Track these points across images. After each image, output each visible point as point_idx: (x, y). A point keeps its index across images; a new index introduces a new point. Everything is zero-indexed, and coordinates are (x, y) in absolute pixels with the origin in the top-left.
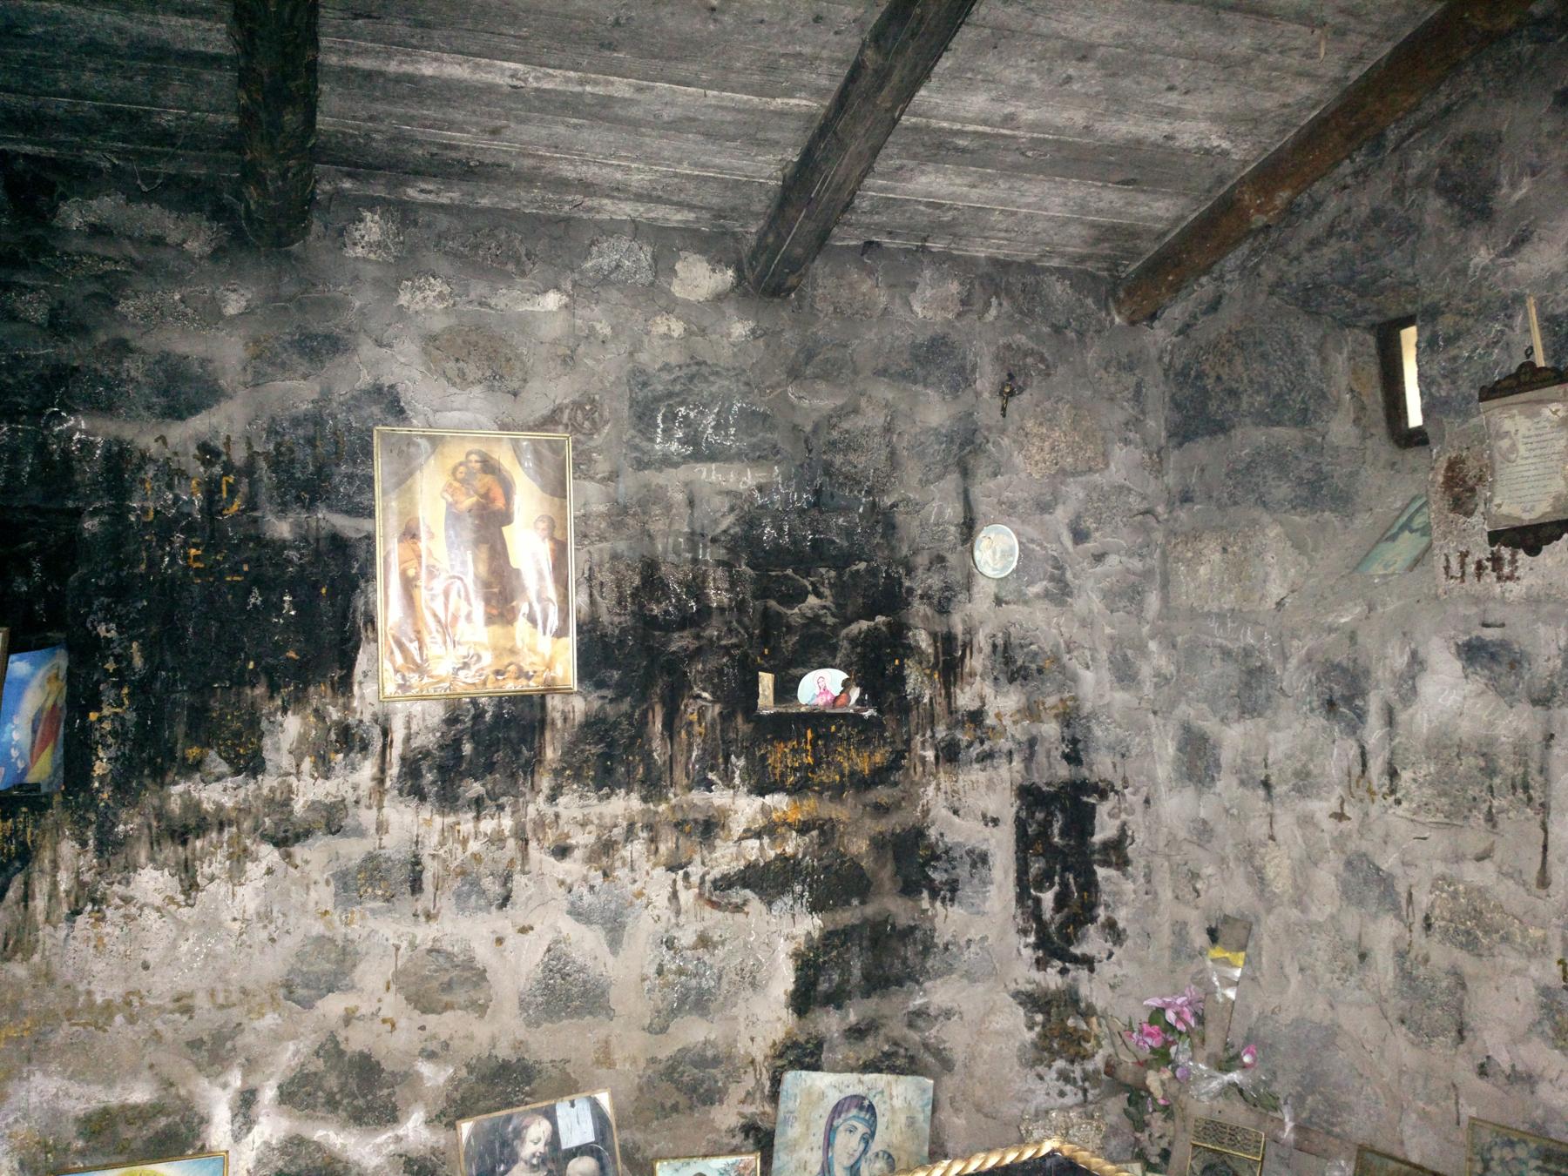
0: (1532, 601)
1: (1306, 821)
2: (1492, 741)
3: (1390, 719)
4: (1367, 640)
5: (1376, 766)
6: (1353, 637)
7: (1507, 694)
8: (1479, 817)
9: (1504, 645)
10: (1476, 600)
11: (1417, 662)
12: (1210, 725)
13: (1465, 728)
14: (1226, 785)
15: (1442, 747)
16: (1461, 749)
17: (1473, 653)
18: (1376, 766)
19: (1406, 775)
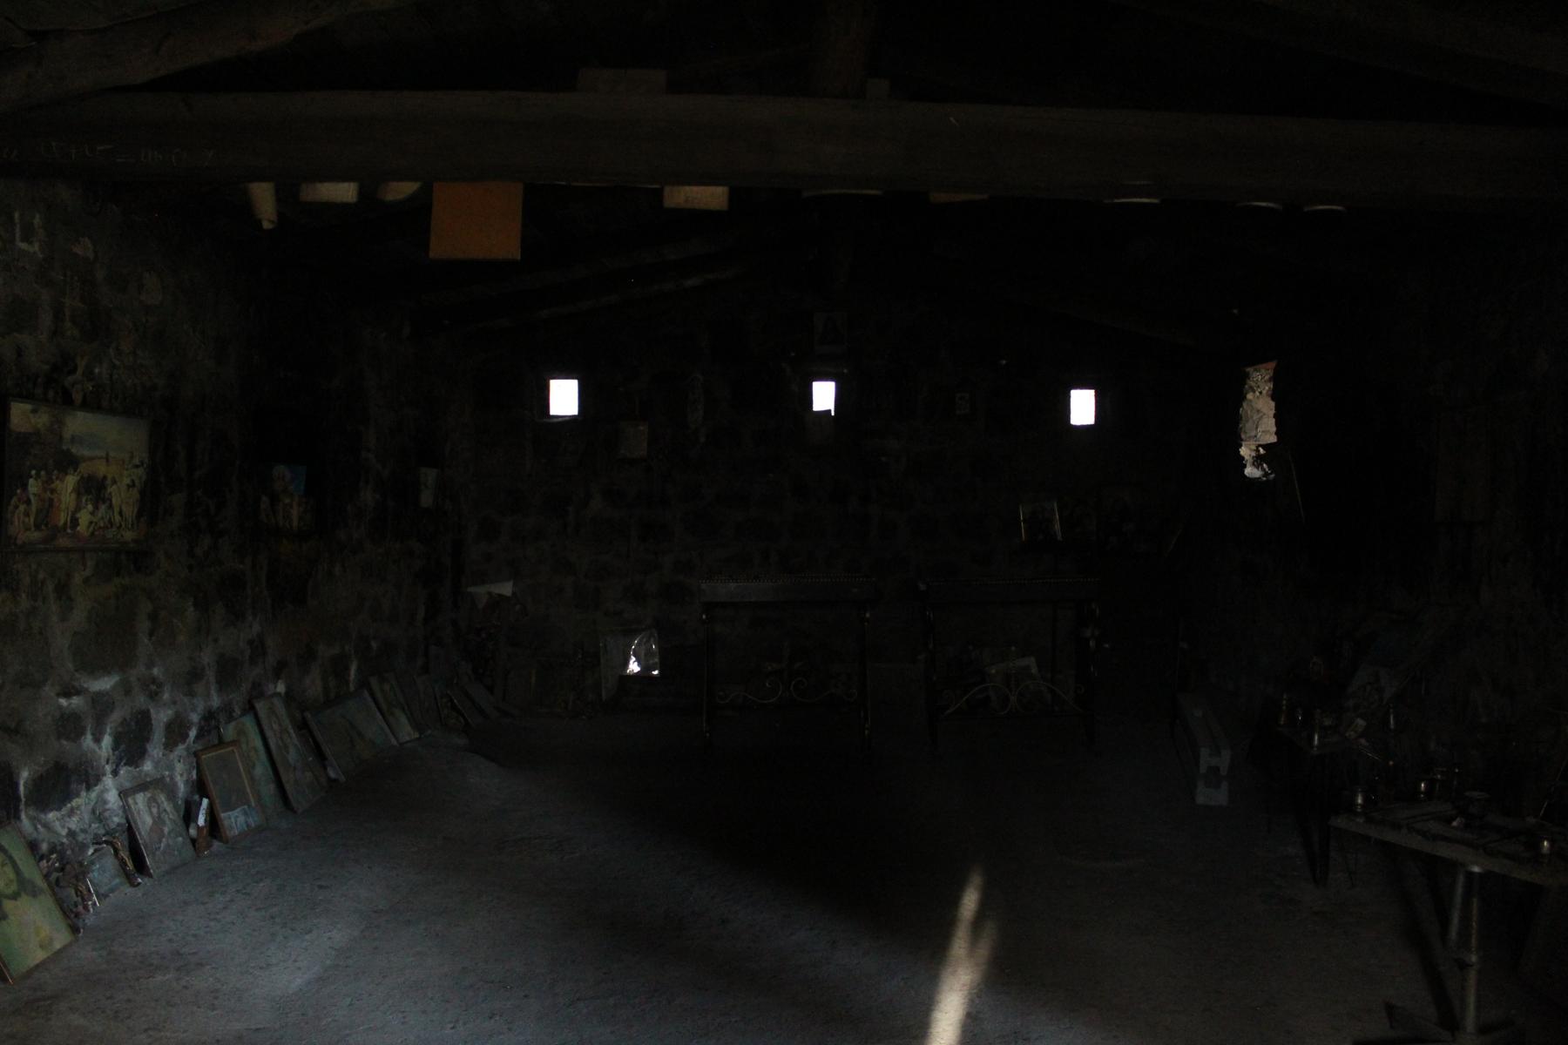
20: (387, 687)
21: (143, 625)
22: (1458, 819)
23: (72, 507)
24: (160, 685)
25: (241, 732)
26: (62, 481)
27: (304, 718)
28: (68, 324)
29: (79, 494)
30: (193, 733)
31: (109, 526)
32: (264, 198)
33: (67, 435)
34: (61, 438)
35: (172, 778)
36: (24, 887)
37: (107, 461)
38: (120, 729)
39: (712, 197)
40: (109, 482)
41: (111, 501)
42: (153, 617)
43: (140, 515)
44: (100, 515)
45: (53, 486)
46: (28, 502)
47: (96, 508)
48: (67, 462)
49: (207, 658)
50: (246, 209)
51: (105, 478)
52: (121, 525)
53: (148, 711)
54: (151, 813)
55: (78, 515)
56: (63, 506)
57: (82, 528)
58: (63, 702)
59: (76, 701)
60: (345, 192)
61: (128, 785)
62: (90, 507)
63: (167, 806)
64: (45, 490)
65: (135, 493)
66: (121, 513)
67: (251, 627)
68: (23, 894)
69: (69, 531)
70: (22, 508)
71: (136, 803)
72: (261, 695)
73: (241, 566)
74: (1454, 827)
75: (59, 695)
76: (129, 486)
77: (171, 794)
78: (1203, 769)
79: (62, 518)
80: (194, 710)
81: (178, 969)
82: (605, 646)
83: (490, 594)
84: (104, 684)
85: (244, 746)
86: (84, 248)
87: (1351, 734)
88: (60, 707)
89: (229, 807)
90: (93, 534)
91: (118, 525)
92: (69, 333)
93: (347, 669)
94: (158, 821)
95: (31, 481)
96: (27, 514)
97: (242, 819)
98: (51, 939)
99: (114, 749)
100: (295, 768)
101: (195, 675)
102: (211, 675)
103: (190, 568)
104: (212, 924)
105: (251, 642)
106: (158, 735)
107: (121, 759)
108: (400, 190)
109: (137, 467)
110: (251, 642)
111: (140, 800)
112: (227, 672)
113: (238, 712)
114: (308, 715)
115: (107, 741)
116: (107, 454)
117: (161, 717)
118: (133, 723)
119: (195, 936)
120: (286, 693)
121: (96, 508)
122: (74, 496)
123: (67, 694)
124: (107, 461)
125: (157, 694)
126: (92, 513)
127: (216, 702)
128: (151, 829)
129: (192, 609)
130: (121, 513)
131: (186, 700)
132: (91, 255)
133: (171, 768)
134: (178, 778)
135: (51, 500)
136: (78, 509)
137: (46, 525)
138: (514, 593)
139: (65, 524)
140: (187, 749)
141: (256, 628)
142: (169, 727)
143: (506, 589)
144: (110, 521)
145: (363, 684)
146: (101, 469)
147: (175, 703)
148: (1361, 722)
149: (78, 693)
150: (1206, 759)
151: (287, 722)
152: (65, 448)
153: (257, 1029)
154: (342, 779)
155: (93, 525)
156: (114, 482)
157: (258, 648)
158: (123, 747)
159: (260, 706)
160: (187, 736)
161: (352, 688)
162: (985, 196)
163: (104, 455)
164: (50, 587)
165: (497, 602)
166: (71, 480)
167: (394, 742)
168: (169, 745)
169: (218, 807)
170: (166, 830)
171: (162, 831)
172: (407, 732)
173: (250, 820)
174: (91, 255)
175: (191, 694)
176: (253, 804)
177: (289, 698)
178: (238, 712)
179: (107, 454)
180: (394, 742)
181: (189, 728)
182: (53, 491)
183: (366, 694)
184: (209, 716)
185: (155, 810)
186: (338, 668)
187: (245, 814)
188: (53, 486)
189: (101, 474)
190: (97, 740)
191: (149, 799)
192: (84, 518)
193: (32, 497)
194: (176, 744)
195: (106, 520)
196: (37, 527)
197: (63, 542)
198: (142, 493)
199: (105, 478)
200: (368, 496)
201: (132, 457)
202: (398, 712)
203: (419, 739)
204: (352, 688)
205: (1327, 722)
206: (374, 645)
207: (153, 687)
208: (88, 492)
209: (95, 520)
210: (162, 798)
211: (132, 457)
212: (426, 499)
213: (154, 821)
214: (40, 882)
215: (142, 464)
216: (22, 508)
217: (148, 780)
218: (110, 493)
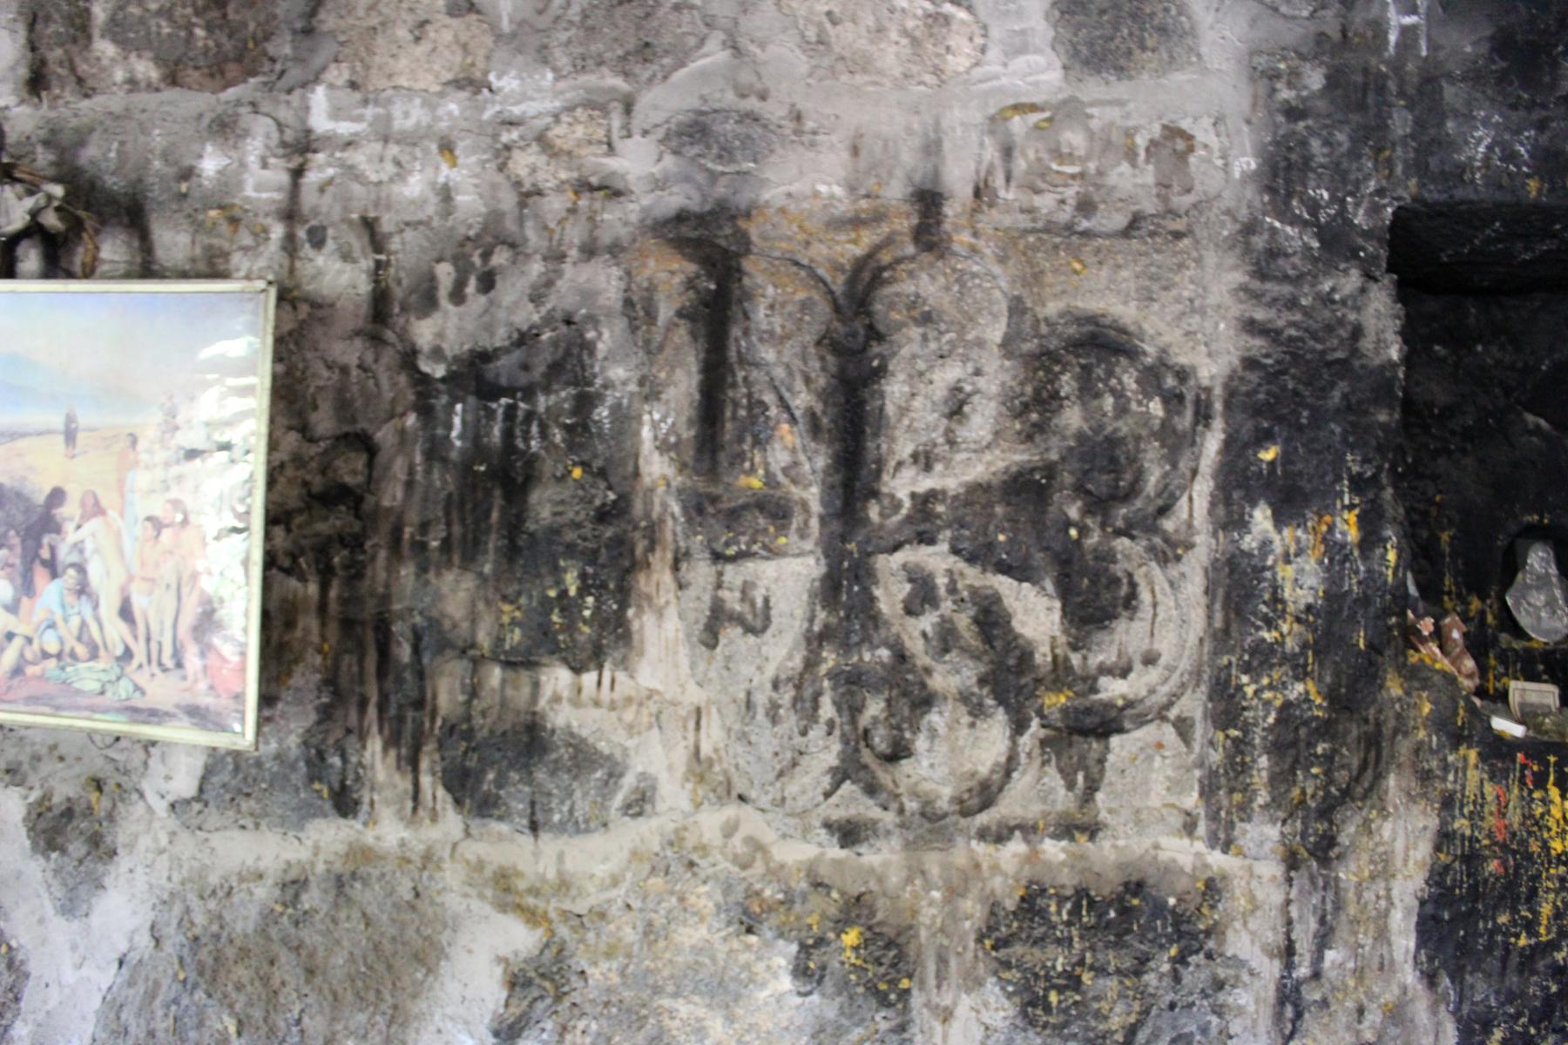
31: (81, 650)
37: (70, 436)
40: (69, 511)
41: (81, 569)
44: (39, 614)
47: (27, 587)
51: (57, 496)
52: (128, 654)
66: (126, 613)
91: (119, 651)
116: (70, 419)
124: (70, 436)
126: (13, 608)
130: (126, 613)
155: (17, 642)
156: (95, 509)
163: (58, 421)
179: (70, 419)
199: (57, 496)
209: (22, 629)
218: (78, 547)
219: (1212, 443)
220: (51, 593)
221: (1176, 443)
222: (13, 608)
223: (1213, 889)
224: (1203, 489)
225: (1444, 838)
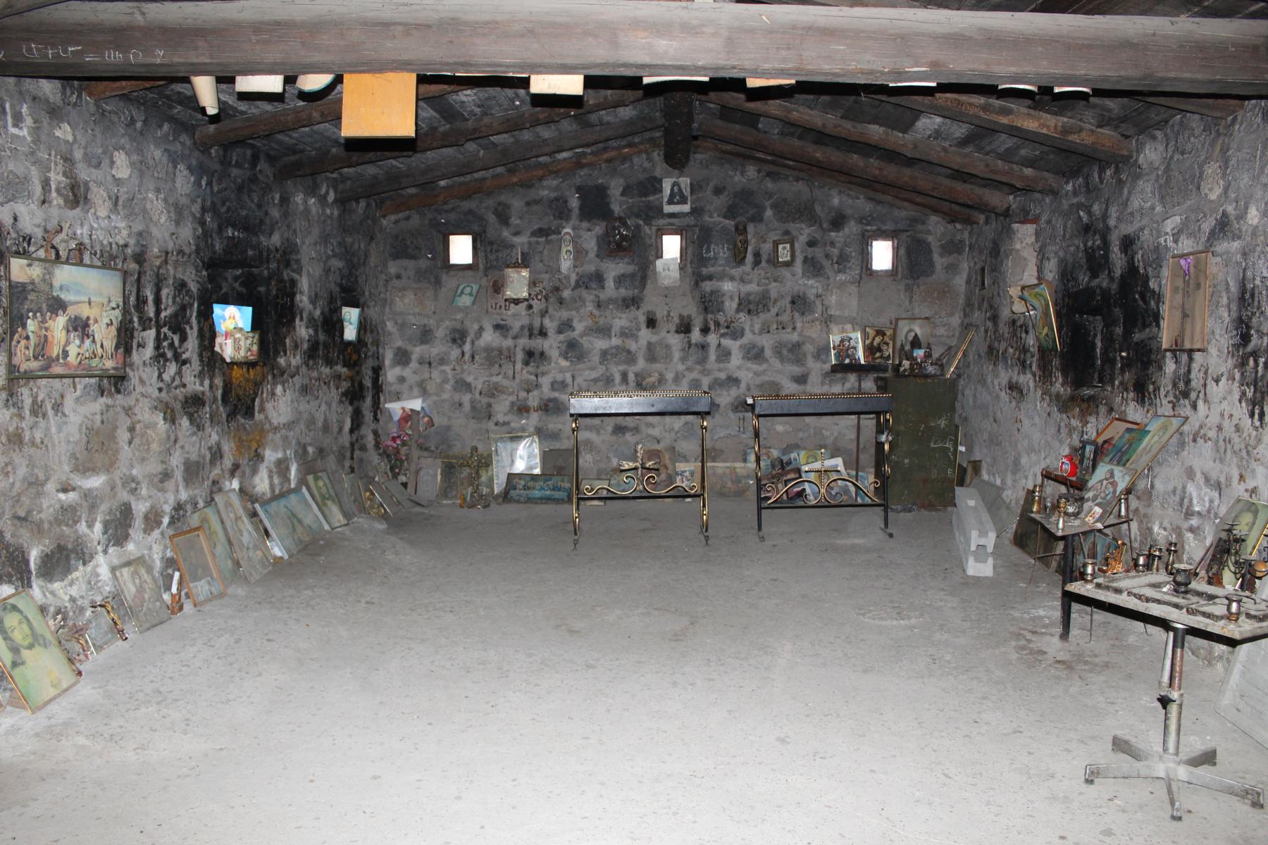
0: (513, 315)
1: (443, 372)
2: (501, 348)
3: (473, 343)
4: (467, 323)
5: (467, 356)
6: (462, 322)
7: (505, 336)
8: (497, 366)
9: (506, 325)
10: (499, 314)
11: (481, 329)
12: (409, 347)
13: (494, 345)
14: (414, 364)
15: (488, 350)
16: (493, 350)
17: (497, 327)
18: (467, 356)
19: (477, 357)
20: (321, 483)
21: (124, 436)
22: (1168, 586)
23: (63, 343)
24: (138, 483)
25: (205, 520)
26: (55, 321)
27: (254, 508)
28: (54, 194)
29: (68, 331)
30: (166, 520)
32: (205, 90)
33: (56, 284)
34: (51, 286)
35: (150, 557)
36: (36, 640)
37: (90, 303)
38: (108, 518)
39: (572, 85)
40: (91, 322)
42: (132, 429)
43: (117, 348)
45: (47, 325)
46: (27, 338)
47: (82, 342)
48: (58, 306)
49: (176, 461)
50: (192, 102)
51: (88, 318)
53: (130, 504)
54: (134, 583)
55: (67, 349)
56: (56, 342)
57: (72, 358)
58: (62, 496)
59: (72, 496)
60: (273, 83)
61: (116, 562)
62: (78, 342)
63: (146, 577)
64: (41, 328)
65: (113, 331)
66: (102, 346)
67: (210, 436)
68: (36, 645)
69: (61, 361)
70: (23, 342)
71: (122, 576)
72: (220, 490)
73: (201, 388)
74: (1164, 593)
75: (58, 491)
76: (108, 325)
77: (150, 569)
78: (973, 548)
79: (55, 351)
80: (165, 502)
81: (159, 703)
82: (496, 450)
83: (403, 409)
84: (95, 482)
85: (207, 532)
86: (64, 132)
87: (1090, 520)
88: (59, 500)
89: (196, 578)
90: (80, 363)
92: (55, 202)
93: (288, 469)
94: (140, 590)
95: (29, 321)
96: (27, 348)
97: (207, 587)
98: (60, 681)
99: (105, 533)
100: (248, 548)
101: (166, 476)
102: (179, 474)
103: (160, 390)
104: (184, 669)
105: (210, 449)
106: (138, 523)
107: (110, 541)
108: (314, 82)
109: (114, 309)
110: (210, 449)
111: (126, 572)
112: (192, 471)
113: (201, 504)
114: (257, 506)
115: (98, 527)
117: (140, 508)
118: (118, 513)
119: (171, 678)
120: (241, 489)
121: (82, 342)
122: (64, 332)
123: (65, 490)
124: (90, 303)
125: (136, 489)
126: (79, 347)
127: (184, 495)
128: (135, 596)
129: (162, 422)
130: (102, 346)
131: (160, 494)
132: (70, 138)
133: (150, 548)
134: (156, 556)
135: (46, 336)
136: (68, 343)
137: (43, 356)
138: (422, 408)
139: (58, 355)
140: (162, 534)
141: (215, 437)
142: (146, 517)
143: (416, 404)
144: (93, 353)
145: (302, 482)
146: (85, 312)
147: (150, 497)
148: (1098, 510)
149: (74, 489)
150: (975, 539)
151: (241, 512)
152: (55, 294)
153: (221, 749)
154: (286, 557)
156: (96, 321)
157: (217, 454)
158: (110, 532)
159: (218, 498)
160: (161, 522)
161: (293, 486)
162: (793, 82)
164: (49, 407)
165: (409, 416)
166: (61, 321)
167: (327, 527)
168: (148, 529)
169: (187, 577)
170: (146, 596)
171: (143, 597)
172: (338, 517)
173: (213, 589)
174: (70, 138)
175: (163, 490)
176: (215, 576)
177: (242, 491)
178: (201, 504)
180: (327, 527)
181: (162, 517)
182: (46, 329)
183: (304, 490)
184: (179, 507)
185: (137, 581)
186: (282, 466)
187: (209, 583)
188: (47, 325)
189: (84, 316)
190: (90, 525)
191: (132, 573)
192: (73, 350)
193: (30, 334)
194: (152, 530)
195: (91, 351)
196: (36, 358)
197: (57, 370)
198: (119, 330)
199: (88, 318)
200: (303, 331)
201: (110, 301)
202: (329, 503)
203: (348, 524)
204: (293, 486)
205: (1071, 509)
206: (310, 450)
207: (133, 485)
208: (75, 329)
209: (82, 352)
210: (143, 571)
211: (110, 301)
212: (350, 333)
213: (137, 590)
214: (49, 636)
215: (118, 307)
216: (23, 342)
217: (132, 558)
219: (196, 305)
220: (88, 342)
221: (192, 305)
222: (79, 347)
223: (203, 393)
224: (195, 314)
225: (224, 381)
